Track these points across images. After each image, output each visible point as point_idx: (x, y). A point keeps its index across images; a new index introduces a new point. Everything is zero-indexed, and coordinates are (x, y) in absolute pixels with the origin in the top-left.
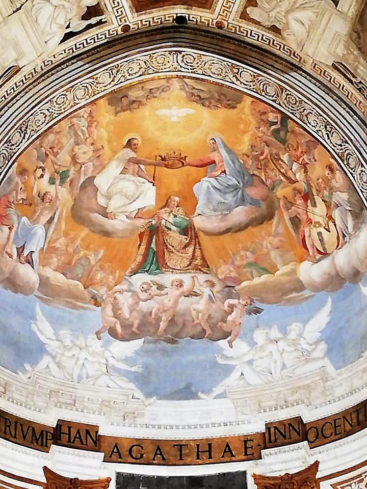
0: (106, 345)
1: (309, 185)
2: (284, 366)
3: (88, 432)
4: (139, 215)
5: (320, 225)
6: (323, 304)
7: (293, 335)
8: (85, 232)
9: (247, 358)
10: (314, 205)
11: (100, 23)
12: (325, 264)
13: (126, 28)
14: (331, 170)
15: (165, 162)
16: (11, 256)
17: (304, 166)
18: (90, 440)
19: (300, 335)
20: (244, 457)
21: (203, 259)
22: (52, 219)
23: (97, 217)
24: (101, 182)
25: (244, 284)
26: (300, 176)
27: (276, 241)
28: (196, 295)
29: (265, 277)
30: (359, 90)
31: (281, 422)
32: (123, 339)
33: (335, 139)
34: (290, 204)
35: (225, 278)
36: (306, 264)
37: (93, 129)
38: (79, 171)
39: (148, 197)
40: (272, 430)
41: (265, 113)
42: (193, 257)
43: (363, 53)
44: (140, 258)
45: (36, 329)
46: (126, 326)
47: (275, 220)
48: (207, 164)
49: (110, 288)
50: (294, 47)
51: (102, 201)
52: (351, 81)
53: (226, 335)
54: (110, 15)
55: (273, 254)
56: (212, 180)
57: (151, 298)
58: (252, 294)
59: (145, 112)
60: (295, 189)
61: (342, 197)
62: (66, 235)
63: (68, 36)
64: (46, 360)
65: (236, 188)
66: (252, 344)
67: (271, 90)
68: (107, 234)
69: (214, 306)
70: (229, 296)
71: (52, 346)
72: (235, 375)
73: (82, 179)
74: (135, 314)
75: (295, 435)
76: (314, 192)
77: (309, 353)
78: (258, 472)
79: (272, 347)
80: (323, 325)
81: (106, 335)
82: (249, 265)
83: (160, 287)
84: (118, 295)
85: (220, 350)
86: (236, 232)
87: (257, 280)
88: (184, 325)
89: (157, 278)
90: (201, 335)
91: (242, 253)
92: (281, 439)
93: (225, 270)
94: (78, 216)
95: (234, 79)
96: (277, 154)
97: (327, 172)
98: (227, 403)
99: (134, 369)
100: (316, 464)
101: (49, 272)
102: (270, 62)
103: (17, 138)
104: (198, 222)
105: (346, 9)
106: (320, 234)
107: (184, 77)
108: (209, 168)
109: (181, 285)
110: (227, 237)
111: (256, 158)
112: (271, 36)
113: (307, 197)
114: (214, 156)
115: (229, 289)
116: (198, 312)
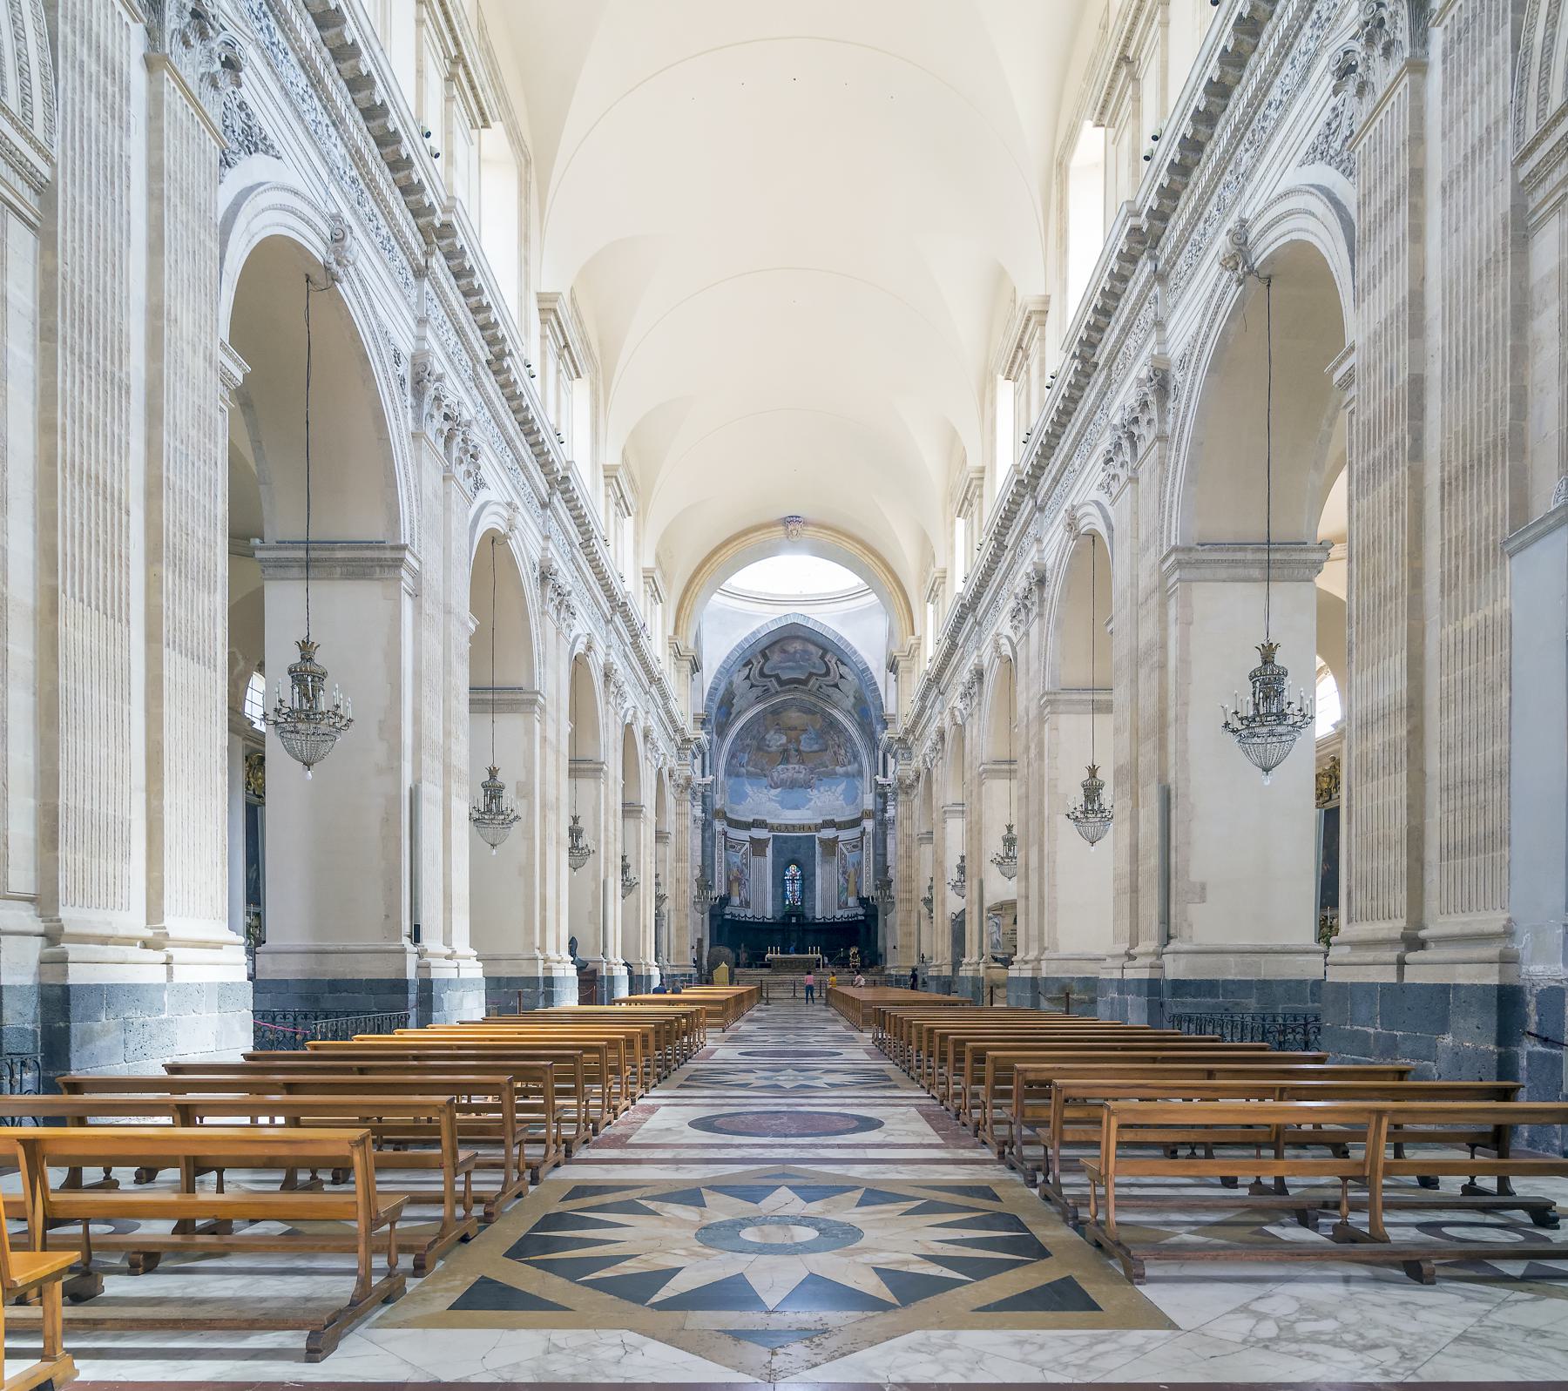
15: (789, 729)
24: (768, 737)
39: (784, 740)
58: (820, 774)
68: (769, 753)
93: (811, 765)
94: (759, 749)
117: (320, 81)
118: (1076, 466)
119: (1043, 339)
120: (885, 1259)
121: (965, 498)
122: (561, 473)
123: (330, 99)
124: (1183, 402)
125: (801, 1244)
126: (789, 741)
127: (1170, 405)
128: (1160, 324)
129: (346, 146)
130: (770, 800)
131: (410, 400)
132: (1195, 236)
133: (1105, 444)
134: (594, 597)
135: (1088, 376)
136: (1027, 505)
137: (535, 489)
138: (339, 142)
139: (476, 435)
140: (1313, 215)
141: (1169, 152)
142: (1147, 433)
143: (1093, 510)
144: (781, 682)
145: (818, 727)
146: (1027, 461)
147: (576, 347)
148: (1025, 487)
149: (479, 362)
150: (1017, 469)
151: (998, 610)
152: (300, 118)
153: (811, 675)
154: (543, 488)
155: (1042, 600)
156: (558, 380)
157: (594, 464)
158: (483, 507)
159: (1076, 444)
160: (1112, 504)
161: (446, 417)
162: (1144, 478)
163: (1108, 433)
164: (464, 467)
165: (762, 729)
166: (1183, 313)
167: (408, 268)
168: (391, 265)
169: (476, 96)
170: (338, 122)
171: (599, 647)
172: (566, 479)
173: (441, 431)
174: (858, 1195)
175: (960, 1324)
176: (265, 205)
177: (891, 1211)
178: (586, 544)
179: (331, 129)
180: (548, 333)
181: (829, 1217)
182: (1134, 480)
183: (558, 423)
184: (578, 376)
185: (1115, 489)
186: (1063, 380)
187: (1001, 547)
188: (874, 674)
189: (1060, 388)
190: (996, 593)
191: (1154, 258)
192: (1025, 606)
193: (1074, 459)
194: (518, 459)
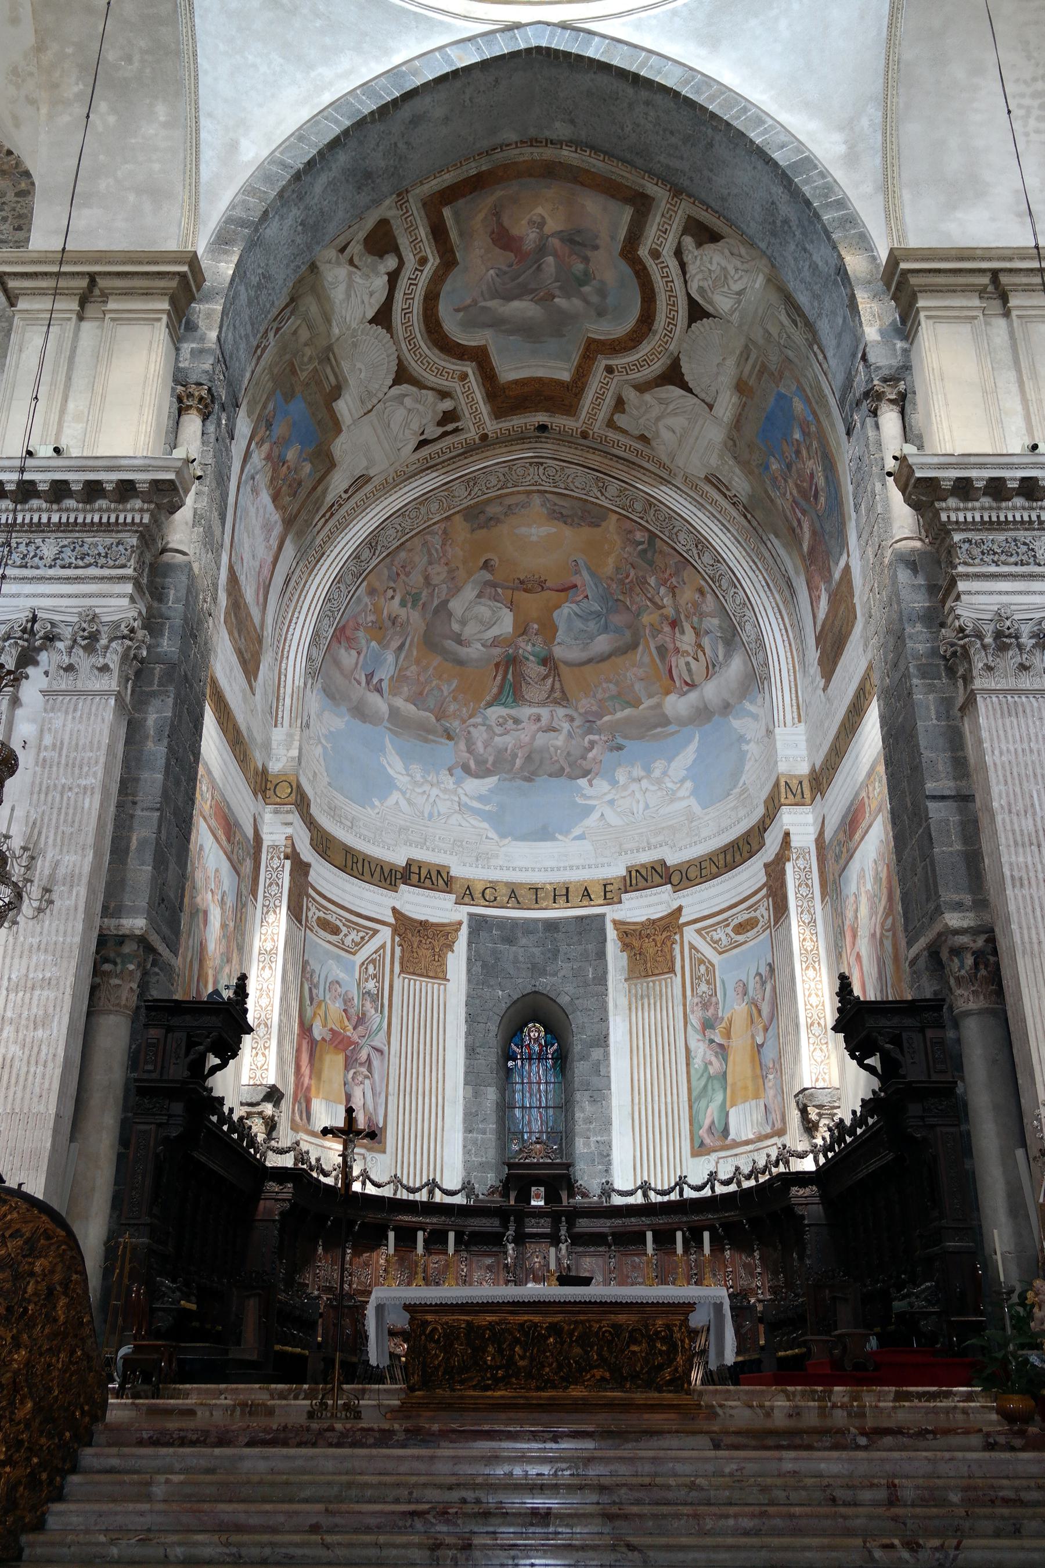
0: (458, 783)
1: (678, 612)
2: (647, 807)
3: (439, 872)
4: (496, 642)
5: (688, 654)
6: (690, 741)
7: (657, 773)
8: (437, 660)
9: (609, 797)
10: (683, 632)
11: (456, 430)
12: (693, 696)
13: (484, 437)
14: (701, 592)
15: (525, 586)
16: (359, 683)
17: (673, 590)
18: (441, 881)
19: (665, 773)
20: (602, 902)
21: (563, 692)
22: (402, 645)
23: (450, 644)
24: (456, 606)
25: (606, 718)
26: (667, 601)
27: (640, 672)
28: (554, 730)
29: (628, 711)
30: (734, 504)
31: (643, 865)
32: (477, 776)
33: (707, 559)
34: (656, 631)
35: (586, 713)
36: (672, 698)
37: (448, 547)
38: (432, 595)
39: (506, 624)
40: (634, 873)
41: (630, 532)
42: (552, 689)
43: (738, 463)
44: (495, 690)
45: (385, 763)
46: (481, 762)
47: (641, 648)
49: (464, 721)
50: (665, 459)
51: (456, 627)
52: (725, 495)
53: (585, 773)
54: (467, 422)
55: (638, 687)
56: (574, 606)
57: (507, 732)
60: (662, 615)
61: (713, 623)
62: (418, 662)
63: (423, 443)
64: (395, 796)
65: (599, 615)
66: (614, 782)
67: (638, 506)
68: (460, 662)
69: (574, 742)
70: (590, 731)
71: (402, 780)
72: (595, 815)
73: (436, 603)
74: (489, 749)
75: (657, 879)
76: (682, 617)
77: (674, 792)
78: (618, 916)
79: (634, 786)
80: (690, 762)
81: (458, 771)
82: (612, 698)
83: (517, 721)
84: (472, 729)
85: (580, 788)
86: (598, 662)
87: (619, 715)
88: (541, 762)
89: (513, 712)
90: (559, 773)
91: (605, 685)
92: (642, 883)
94: (431, 642)
95: (599, 494)
96: (644, 577)
97: (697, 596)
98: (586, 845)
99: (487, 808)
100: (680, 909)
101: (399, 702)
102: (639, 475)
103: (366, 554)
104: (558, 652)
105: (720, 415)
106: (688, 664)
107: (546, 492)
108: (571, 592)
109: (538, 719)
110: (588, 668)
111: (621, 582)
112: (639, 446)
113: (674, 624)
114: (576, 580)
115: (590, 724)
116: (556, 748)
126: (522, 629)
130: (463, 808)
145: (609, 566)
153: (593, 349)
165: (438, 574)
188: (839, 174)
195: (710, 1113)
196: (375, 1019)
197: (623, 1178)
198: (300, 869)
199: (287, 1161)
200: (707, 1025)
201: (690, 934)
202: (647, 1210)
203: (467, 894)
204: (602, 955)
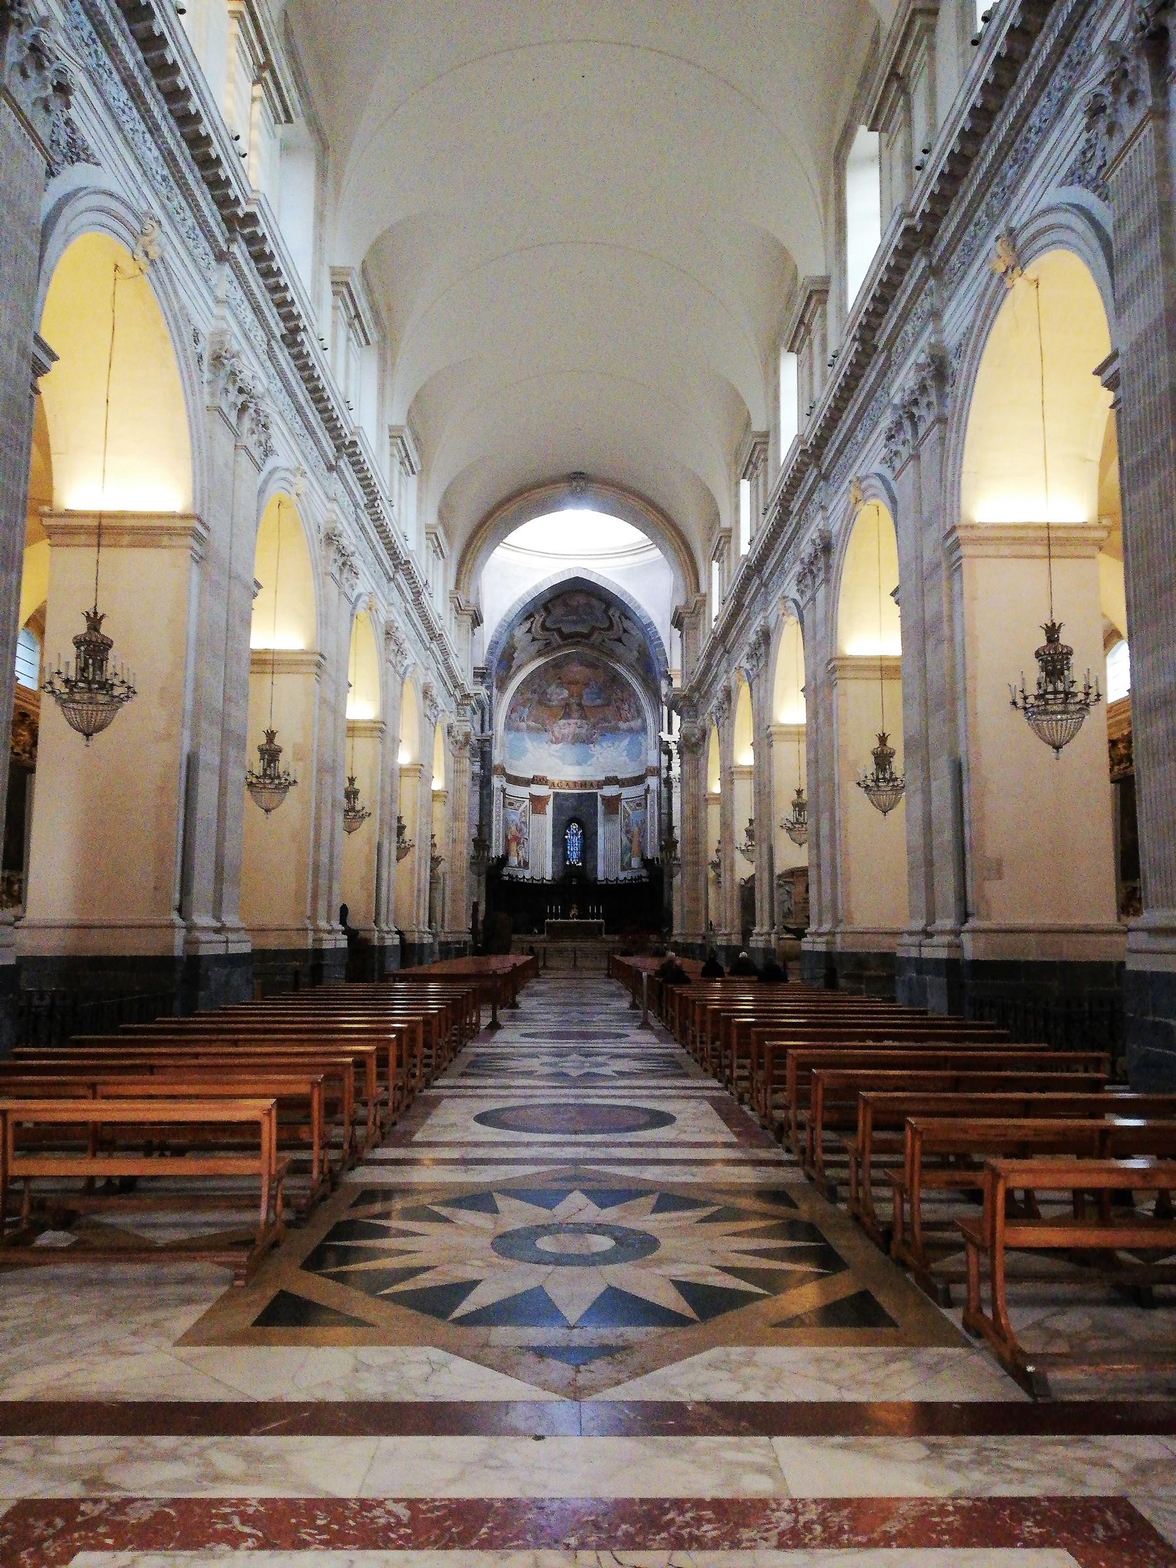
15: (570, 683)
24: (549, 691)
39: (566, 693)
46: (557, 739)
48: (587, 685)
59: (565, 669)
64: (529, 754)
90: (584, 742)
115: (594, 726)
117: (140, 94)
118: (859, 438)
119: (824, 316)
120: (685, 1271)
121: (750, 461)
122: (350, 438)
123: (149, 110)
124: (961, 389)
125: (597, 1254)
126: (571, 695)
127: (948, 389)
128: (935, 315)
129: (160, 149)
130: (551, 755)
131: (207, 376)
132: (966, 238)
133: (886, 422)
134: (377, 555)
135: (869, 356)
136: (812, 475)
137: (324, 455)
138: (153, 147)
139: (267, 407)
140: (1073, 230)
141: (937, 162)
142: (928, 417)
143: (877, 482)
144: (564, 637)
146: (810, 433)
147: (367, 316)
148: (810, 456)
149: (274, 337)
150: (800, 439)
151: (784, 573)
152: (120, 129)
154: (331, 452)
155: (828, 567)
156: (348, 347)
157: (380, 424)
158: (271, 473)
159: (858, 419)
160: (895, 478)
161: (241, 391)
162: (925, 456)
163: (889, 411)
164: (255, 437)
166: (958, 305)
167: (211, 253)
168: (196, 251)
169: (281, 96)
170: (154, 130)
171: (381, 606)
172: (354, 444)
173: (235, 404)
174: (652, 1200)
175: (759, 1341)
176: (83, 208)
177: (687, 1218)
178: (371, 504)
179: (148, 136)
180: (340, 303)
181: (625, 1224)
182: (916, 457)
183: (347, 388)
184: (368, 343)
185: (898, 464)
186: (845, 359)
187: (785, 513)
188: (658, 628)
189: (841, 367)
190: (783, 555)
191: (929, 255)
192: (811, 572)
193: (857, 433)
194: (308, 426)
195: (626, 859)
196: (525, 830)
197: (600, 877)
198: (504, 790)
199: (507, 878)
200: (627, 832)
201: (624, 803)
202: (607, 885)
203: (553, 785)
204: (596, 805)
